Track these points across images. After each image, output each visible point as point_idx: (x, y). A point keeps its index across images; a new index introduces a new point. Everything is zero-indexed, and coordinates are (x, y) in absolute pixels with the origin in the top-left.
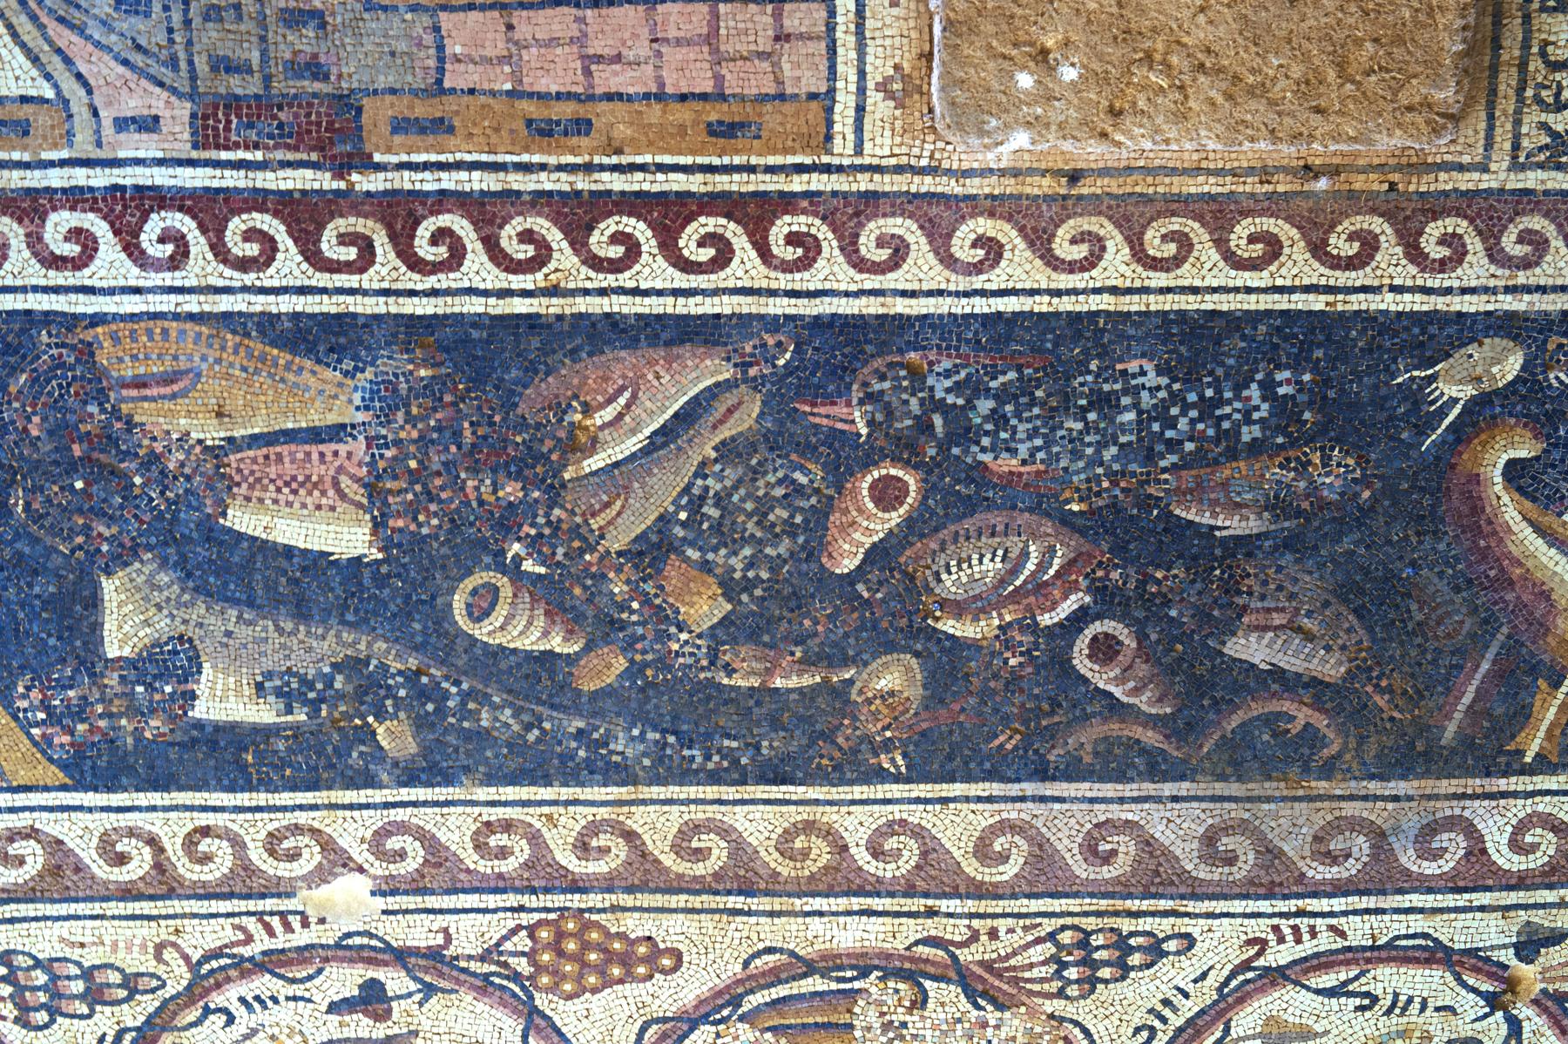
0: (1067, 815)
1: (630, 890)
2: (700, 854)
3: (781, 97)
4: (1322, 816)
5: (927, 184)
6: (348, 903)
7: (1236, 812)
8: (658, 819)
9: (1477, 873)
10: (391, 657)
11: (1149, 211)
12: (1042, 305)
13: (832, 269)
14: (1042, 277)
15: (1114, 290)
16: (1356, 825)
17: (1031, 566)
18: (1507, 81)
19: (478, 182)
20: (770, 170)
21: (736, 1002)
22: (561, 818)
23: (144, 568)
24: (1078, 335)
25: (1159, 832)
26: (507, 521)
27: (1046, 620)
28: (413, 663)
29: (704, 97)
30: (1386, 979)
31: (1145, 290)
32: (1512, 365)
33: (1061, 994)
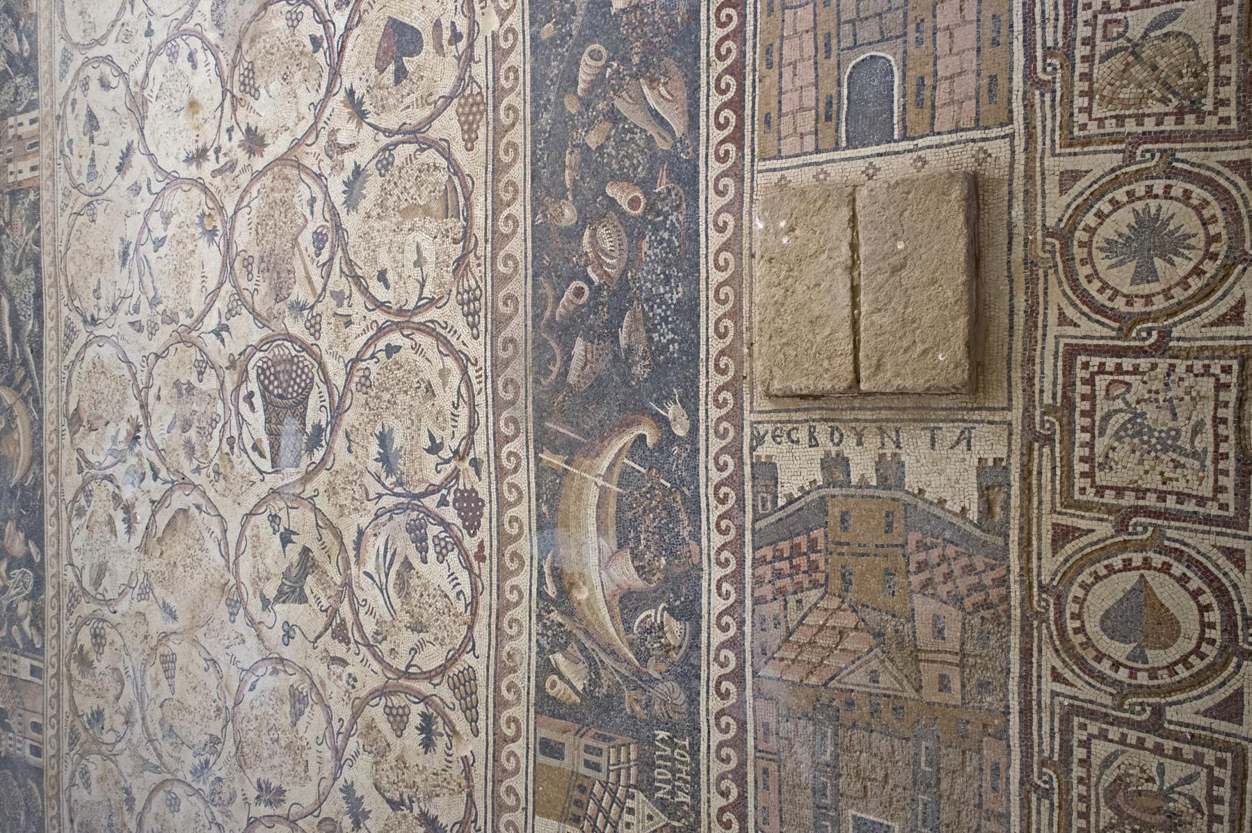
0: (521, 287)
1: (494, 128)
2: (506, 153)
3: (780, 139)
4: (520, 382)
5: (747, 200)
6: (490, 23)
7: (521, 350)
8: (519, 135)
11: (737, 287)
12: (702, 251)
13: (716, 168)
14: (713, 249)
15: (708, 277)
16: (517, 394)
17: (608, 261)
18: (784, 416)
19: (749, 29)
20: (753, 139)
21: (455, 174)
22: (519, 99)
24: (691, 267)
25: (515, 321)
26: (625, 60)
27: (589, 269)
28: (574, 33)
29: (780, 110)
30: (464, 411)
31: (707, 289)
32: (680, 432)
33: (458, 293)
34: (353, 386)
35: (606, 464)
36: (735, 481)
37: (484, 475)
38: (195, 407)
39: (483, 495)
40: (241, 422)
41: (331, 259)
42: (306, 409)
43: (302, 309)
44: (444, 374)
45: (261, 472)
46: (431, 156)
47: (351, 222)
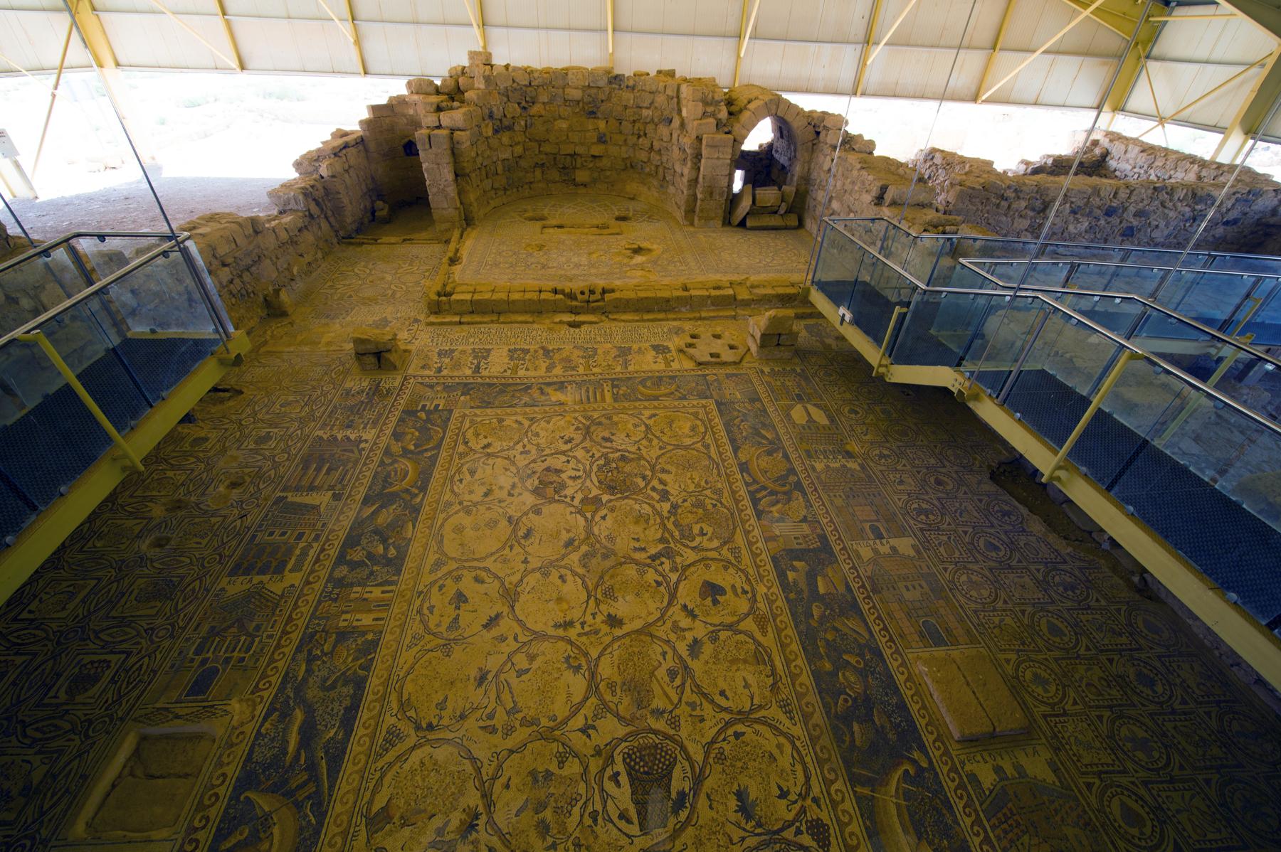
0: (813, 698)
6: (762, 589)
9: (828, 783)
10: (805, 595)
16: (830, 755)
22: (786, 617)
23: (807, 568)
30: (799, 768)
32: (925, 765)
34: (711, 760)
35: (893, 789)
36: (961, 786)
37: (823, 807)
38: (552, 790)
39: (826, 820)
40: (605, 796)
41: (683, 684)
42: (670, 780)
43: (664, 712)
44: (779, 746)
45: (629, 837)
46: (741, 637)
47: (695, 665)
